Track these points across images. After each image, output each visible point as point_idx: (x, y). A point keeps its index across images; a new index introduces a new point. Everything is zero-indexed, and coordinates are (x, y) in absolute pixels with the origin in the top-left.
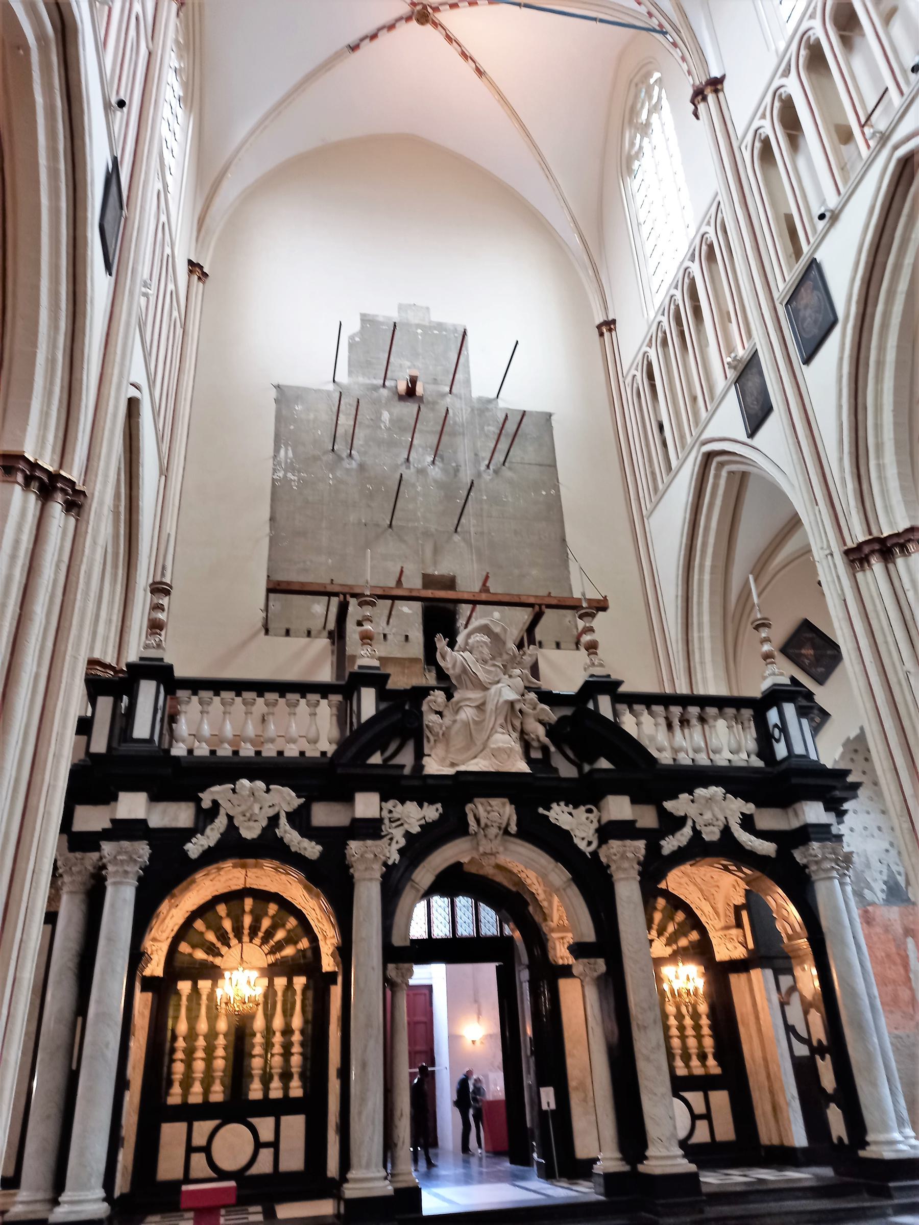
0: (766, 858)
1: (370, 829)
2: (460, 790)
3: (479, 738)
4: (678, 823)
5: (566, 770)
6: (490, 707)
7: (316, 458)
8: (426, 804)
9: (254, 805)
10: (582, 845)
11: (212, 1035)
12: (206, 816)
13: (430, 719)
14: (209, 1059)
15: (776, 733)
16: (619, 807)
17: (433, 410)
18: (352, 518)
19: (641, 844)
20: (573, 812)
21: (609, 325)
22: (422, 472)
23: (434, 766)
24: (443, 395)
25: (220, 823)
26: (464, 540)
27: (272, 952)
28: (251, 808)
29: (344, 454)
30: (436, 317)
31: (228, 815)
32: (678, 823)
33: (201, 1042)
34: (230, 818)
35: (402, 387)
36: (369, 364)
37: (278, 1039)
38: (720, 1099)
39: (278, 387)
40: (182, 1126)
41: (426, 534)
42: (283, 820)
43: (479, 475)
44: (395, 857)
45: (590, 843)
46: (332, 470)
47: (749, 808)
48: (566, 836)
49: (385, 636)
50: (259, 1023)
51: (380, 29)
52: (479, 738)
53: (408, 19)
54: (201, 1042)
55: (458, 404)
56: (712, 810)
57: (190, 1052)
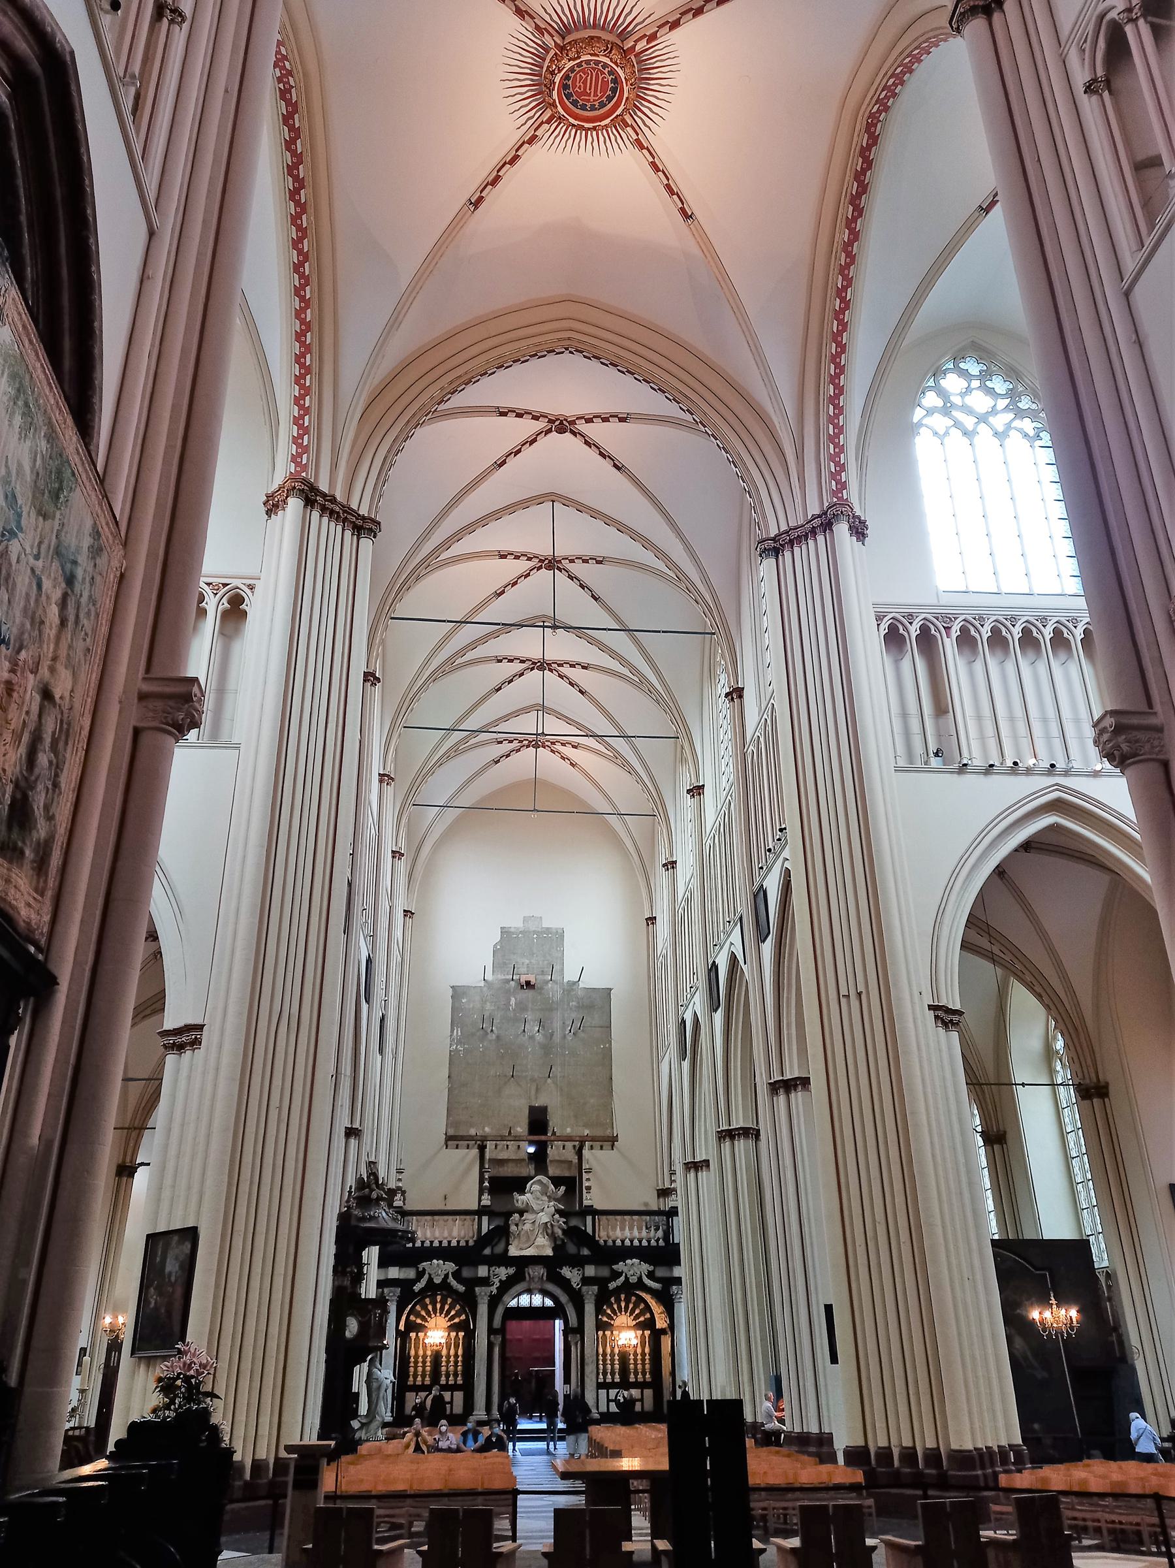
2: (523, 1262)
3: (533, 1237)
4: (620, 1274)
5: (571, 1249)
7: (473, 1034)
9: (439, 1269)
11: (425, 1356)
12: (420, 1275)
13: (513, 1228)
14: (424, 1366)
16: (590, 1271)
17: (540, 994)
18: (492, 1073)
19: (596, 1288)
21: (652, 920)
22: (532, 1038)
23: (513, 1251)
24: (547, 982)
25: (426, 1276)
27: (450, 1320)
32: (620, 1274)
33: (420, 1359)
36: (505, 964)
37: (452, 1359)
38: (648, 1393)
41: (533, 1080)
43: (564, 1037)
44: (495, 1291)
46: (482, 1042)
47: (651, 1268)
50: (444, 1352)
52: (533, 1237)
54: (420, 1359)
55: (557, 987)
56: (634, 1269)
57: (416, 1362)
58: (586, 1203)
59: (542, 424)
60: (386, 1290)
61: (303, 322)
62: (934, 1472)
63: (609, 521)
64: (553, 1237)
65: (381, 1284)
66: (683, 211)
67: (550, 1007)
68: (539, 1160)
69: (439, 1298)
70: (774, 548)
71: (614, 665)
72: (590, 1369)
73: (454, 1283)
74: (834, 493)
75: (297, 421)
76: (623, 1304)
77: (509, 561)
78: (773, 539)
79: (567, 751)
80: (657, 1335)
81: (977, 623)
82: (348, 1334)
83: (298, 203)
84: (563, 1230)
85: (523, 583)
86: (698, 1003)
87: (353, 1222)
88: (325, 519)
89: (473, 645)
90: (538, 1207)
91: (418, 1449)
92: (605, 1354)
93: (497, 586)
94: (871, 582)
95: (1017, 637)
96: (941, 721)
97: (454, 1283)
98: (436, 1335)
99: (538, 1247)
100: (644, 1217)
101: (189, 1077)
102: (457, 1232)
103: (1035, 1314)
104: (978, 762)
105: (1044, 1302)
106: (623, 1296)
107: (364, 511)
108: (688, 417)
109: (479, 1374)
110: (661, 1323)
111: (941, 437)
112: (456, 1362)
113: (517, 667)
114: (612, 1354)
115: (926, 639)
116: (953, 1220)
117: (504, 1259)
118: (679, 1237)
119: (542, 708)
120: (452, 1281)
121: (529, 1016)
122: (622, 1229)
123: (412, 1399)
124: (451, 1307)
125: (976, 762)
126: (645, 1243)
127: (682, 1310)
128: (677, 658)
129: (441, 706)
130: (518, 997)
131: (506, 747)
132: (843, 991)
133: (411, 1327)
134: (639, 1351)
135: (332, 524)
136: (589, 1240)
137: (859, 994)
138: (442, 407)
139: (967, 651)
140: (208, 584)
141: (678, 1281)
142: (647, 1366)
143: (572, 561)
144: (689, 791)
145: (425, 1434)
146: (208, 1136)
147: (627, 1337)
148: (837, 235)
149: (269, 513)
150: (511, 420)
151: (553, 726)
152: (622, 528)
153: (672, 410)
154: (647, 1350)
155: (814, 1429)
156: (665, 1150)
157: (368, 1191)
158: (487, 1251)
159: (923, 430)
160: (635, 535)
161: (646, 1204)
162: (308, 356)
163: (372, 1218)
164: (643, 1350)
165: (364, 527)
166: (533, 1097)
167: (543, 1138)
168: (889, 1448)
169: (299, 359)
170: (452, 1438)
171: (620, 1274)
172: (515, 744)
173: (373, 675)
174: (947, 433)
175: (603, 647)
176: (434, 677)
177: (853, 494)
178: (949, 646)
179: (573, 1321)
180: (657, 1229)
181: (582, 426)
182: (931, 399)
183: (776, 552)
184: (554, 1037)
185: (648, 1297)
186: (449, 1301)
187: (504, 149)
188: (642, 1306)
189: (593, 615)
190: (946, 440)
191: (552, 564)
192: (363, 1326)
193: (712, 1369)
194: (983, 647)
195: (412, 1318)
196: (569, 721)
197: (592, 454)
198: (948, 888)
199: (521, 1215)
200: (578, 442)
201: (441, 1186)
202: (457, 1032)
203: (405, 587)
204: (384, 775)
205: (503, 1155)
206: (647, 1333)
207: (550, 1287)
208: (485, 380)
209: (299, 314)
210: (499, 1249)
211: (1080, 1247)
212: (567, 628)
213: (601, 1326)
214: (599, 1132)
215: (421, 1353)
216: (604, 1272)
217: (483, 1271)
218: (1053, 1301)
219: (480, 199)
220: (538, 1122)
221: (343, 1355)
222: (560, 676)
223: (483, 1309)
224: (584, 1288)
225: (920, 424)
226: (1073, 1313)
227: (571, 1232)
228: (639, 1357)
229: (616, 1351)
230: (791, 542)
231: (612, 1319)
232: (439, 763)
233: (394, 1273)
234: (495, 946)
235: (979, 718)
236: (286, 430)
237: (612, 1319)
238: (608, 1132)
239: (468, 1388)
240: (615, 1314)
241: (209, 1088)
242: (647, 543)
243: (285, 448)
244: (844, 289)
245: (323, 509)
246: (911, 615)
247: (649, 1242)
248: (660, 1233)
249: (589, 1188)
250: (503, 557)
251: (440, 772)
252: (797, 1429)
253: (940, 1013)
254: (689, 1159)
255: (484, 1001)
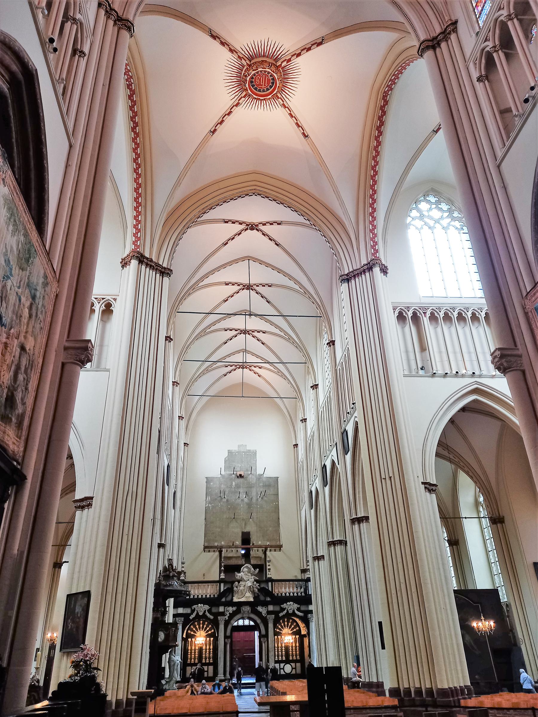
0: (301, 617)
1: (223, 614)
2: (240, 605)
3: (244, 593)
4: (284, 609)
5: (262, 598)
7: (216, 499)
9: (201, 608)
11: (195, 650)
12: (193, 611)
13: (235, 589)
14: (195, 654)
16: (271, 608)
18: (225, 516)
19: (274, 616)
21: (296, 445)
22: (243, 500)
23: (235, 600)
24: (249, 475)
25: (196, 612)
30: (248, 448)
32: (284, 609)
33: (193, 651)
36: (230, 467)
37: (208, 651)
38: (298, 665)
39: (206, 478)
40: (190, 667)
41: (243, 520)
43: (257, 500)
44: (227, 618)
46: (220, 503)
47: (299, 606)
50: (204, 648)
52: (244, 593)
55: (253, 477)
56: (291, 606)
57: (191, 653)
58: (268, 576)
59: (243, 226)
60: (177, 619)
61: (138, 184)
62: (430, 699)
63: (274, 268)
64: (253, 592)
65: (175, 616)
66: (303, 134)
67: (250, 486)
68: (247, 556)
69: (201, 622)
70: (347, 278)
71: (277, 331)
72: (271, 654)
73: (208, 615)
74: (373, 254)
75: (135, 226)
76: (286, 623)
77: (230, 286)
78: (347, 275)
79: (257, 370)
80: (302, 637)
81: (438, 311)
82: (159, 640)
83: (135, 133)
84: (258, 589)
85: (236, 296)
86: (318, 483)
87: (162, 587)
88: (148, 269)
89: (214, 324)
90: (247, 579)
91: (192, 693)
92: (278, 647)
93: (224, 297)
94: (389, 293)
95: (456, 316)
96: (424, 354)
97: (208, 615)
98: (200, 639)
99: (246, 597)
100: (295, 583)
101: (87, 521)
102: (209, 591)
103: (474, 624)
104: (440, 372)
105: (479, 619)
106: (286, 620)
107: (165, 265)
108: (308, 222)
109: (220, 658)
110: (304, 632)
111: (419, 229)
112: (210, 652)
113: (234, 333)
114: (281, 647)
115: (415, 318)
116: (436, 581)
117: (231, 603)
118: (311, 591)
119: (245, 351)
120: (207, 613)
121: (241, 490)
122: (285, 588)
123: (189, 670)
124: (207, 626)
125: (440, 372)
126: (295, 594)
127: (313, 625)
128: (305, 328)
129: (201, 350)
130: (236, 482)
131: (229, 369)
132: (383, 477)
133: (189, 636)
134: (294, 645)
135: (151, 271)
136: (270, 594)
137: (390, 478)
138: (199, 220)
139: (434, 323)
140: (96, 298)
141: (311, 612)
142: (298, 652)
143: (258, 286)
144: (311, 387)
145: (196, 686)
146: (95, 548)
147: (288, 639)
148: (371, 143)
149: (123, 267)
150: (230, 225)
151: (250, 359)
152: (280, 271)
153: (301, 219)
154: (297, 645)
155: (375, 680)
156: (304, 551)
157: (169, 573)
158: (223, 600)
159: (411, 227)
160: (285, 274)
161: (296, 576)
162: (140, 198)
163: (170, 585)
164: (296, 645)
165: (165, 272)
166: (243, 528)
167: (248, 546)
168: (409, 688)
169: (136, 199)
170: (209, 688)
171: (284, 609)
172: (234, 367)
173: (169, 337)
174: (422, 228)
175: (272, 323)
176: (197, 337)
177: (381, 255)
178: (425, 321)
179: (263, 632)
180: (301, 588)
181: (261, 227)
182: (414, 213)
183: (348, 280)
184: (253, 500)
185: (297, 620)
186: (206, 623)
187: (225, 109)
188: (295, 624)
189: (267, 309)
190: (422, 231)
191: (249, 287)
192: (167, 636)
193: (327, 653)
194: (441, 321)
195: (189, 632)
196: (258, 356)
197: (266, 239)
198: (429, 429)
199: (239, 583)
200: (259, 234)
201: (201, 569)
202: (209, 498)
203: (184, 298)
204: (175, 382)
205: (230, 555)
206: (297, 636)
207: (253, 616)
208: (218, 208)
209: (136, 180)
210: (229, 599)
211: (494, 592)
212: (256, 315)
213: (276, 634)
214: (274, 543)
215: (193, 648)
216: (277, 608)
217: (221, 609)
218: (482, 618)
219: (215, 130)
220: (246, 539)
221: (157, 650)
222: (253, 336)
223: (222, 627)
224: (268, 616)
225: (410, 224)
226: (492, 623)
227: (263, 591)
228: (294, 648)
229: (283, 645)
230: (354, 276)
231: (281, 630)
232: (199, 376)
233: (180, 610)
234: (225, 459)
235: (440, 352)
236: (131, 230)
237: (281, 630)
238: (278, 543)
239: (215, 664)
240: (283, 628)
241: (96, 526)
242: (291, 278)
243: (130, 238)
244: (375, 166)
245: (147, 265)
246: (408, 307)
247: (297, 594)
248: (302, 590)
249: (269, 569)
250: (227, 284)
251: (200, 380)
252: (367, 680)
253: (427, 486)
254: (315, 555)
255: (221, 484)
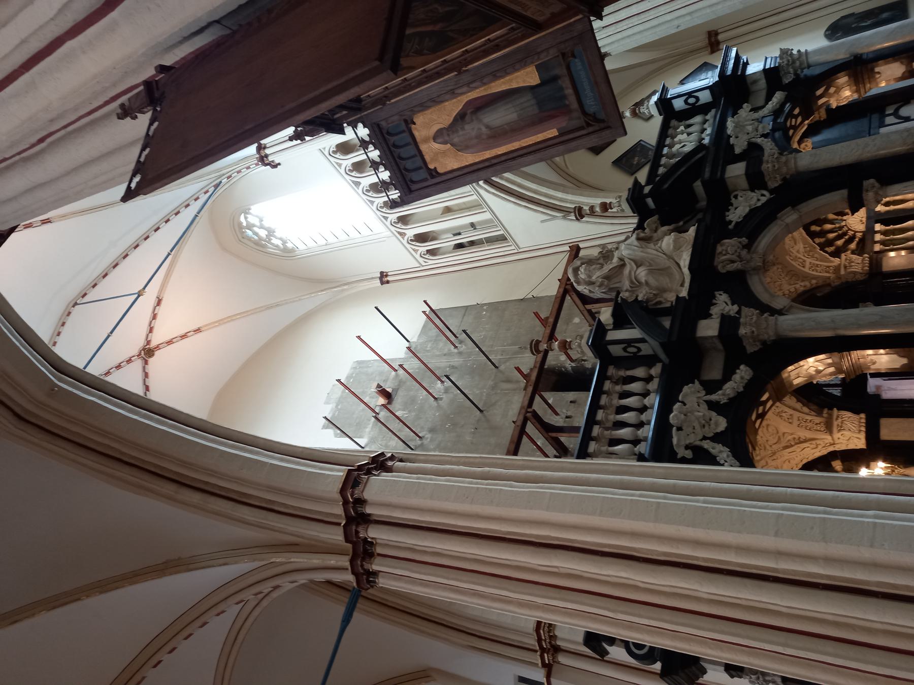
6: (639, 254)
8: (714, 301)
10: (764, 199)
15: (692, 100)
17: (405, 382)
18: (468, 438)
20: (735, 206)
25: (707, 445)
26: (505, 362)
28: (698, 418)
29: (419, 442)
31: (701, 440)
34: (705, 438)
35: (382, 401)
41: (493, 388)
42: (713, 397)
43: (460, 353)
45: (763, 195)
48: (753, 212)
49: (567, 417)
51: (144, 368)
53: (146, 363)
73: (730, 389)
